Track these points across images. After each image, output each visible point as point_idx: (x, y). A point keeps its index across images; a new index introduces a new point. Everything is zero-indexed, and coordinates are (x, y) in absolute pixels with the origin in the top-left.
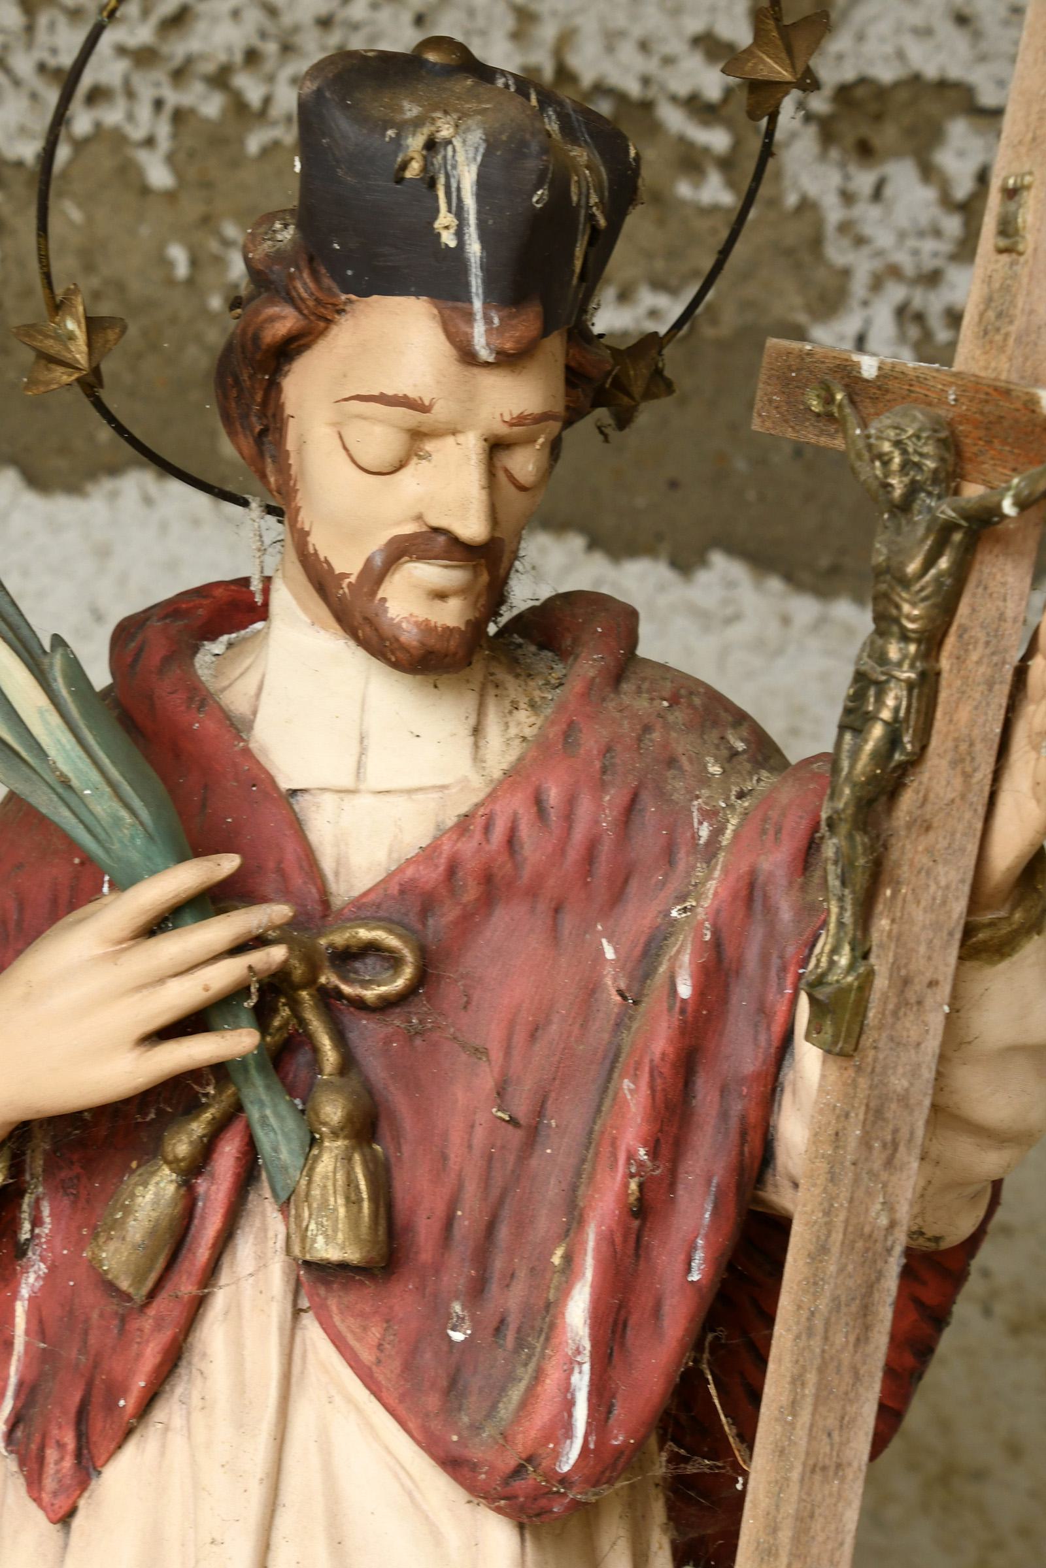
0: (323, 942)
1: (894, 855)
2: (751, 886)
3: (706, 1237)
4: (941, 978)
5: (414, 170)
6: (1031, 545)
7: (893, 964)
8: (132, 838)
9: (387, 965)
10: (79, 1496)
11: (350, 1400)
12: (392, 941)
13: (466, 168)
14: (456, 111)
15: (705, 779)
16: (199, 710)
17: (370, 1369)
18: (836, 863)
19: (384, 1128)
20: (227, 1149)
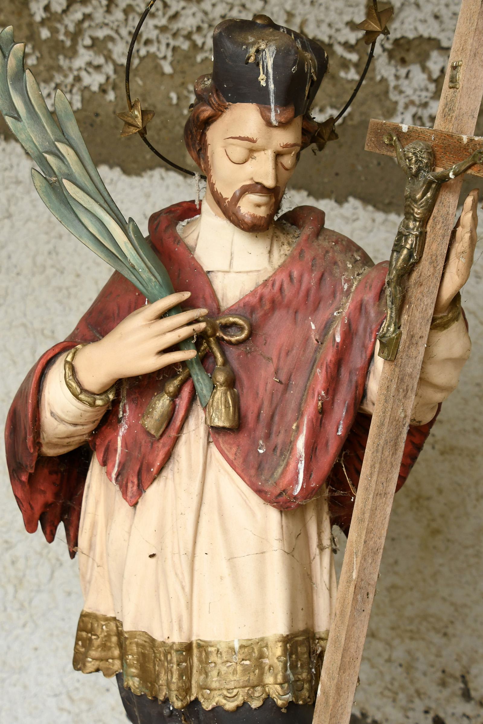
0: (218, 322)
1: (410, 294)
2: (361, 305)
3: (344, 420)
4: (424, 335)
5: (252, 58)
6: (459, 189)
7: (408, 330)
8: (155, 286)
9: (239, 330)
10: (139, 498)
11: (226, 471)
12: (241, 322)
13: (270, 59)
14: (267, 40)
15: (346, 269)
16: (177, 244)
17: (232, 461)
18: (390, 296)
19: (237, 384)
20: (186, 389)
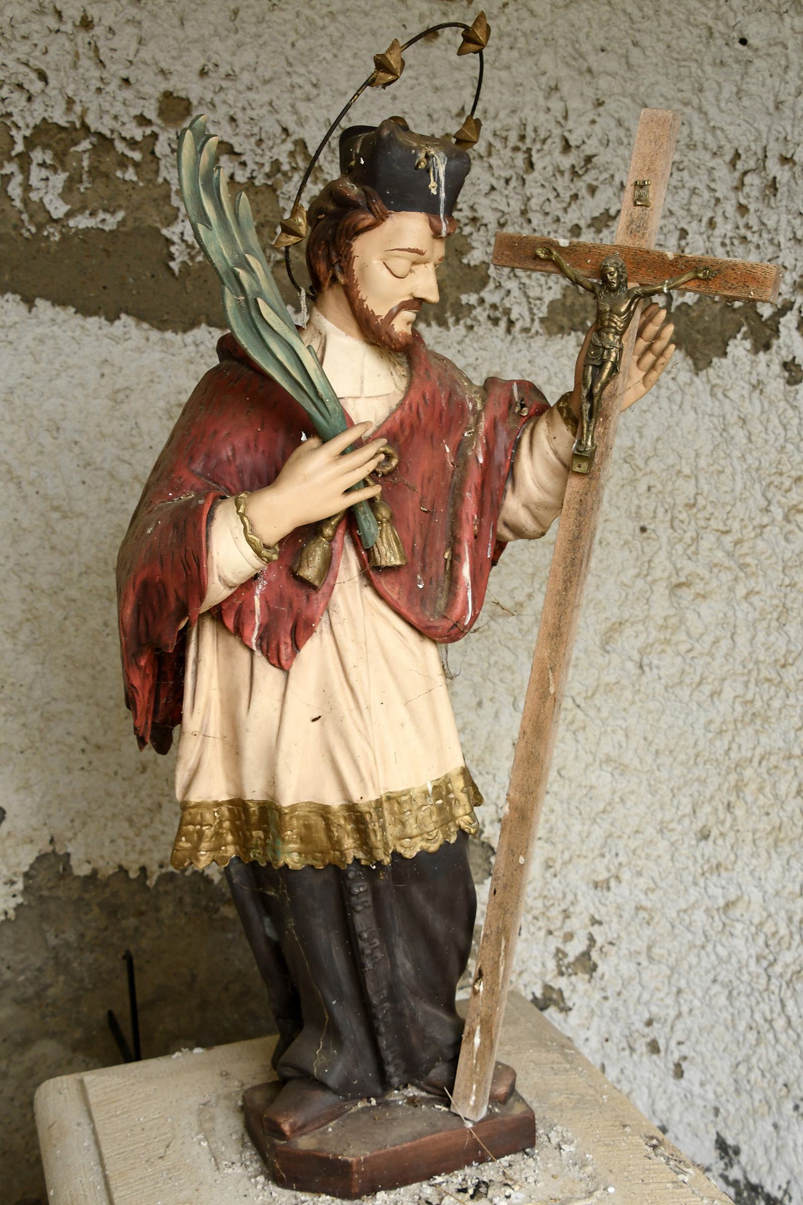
5: (423, 165)
